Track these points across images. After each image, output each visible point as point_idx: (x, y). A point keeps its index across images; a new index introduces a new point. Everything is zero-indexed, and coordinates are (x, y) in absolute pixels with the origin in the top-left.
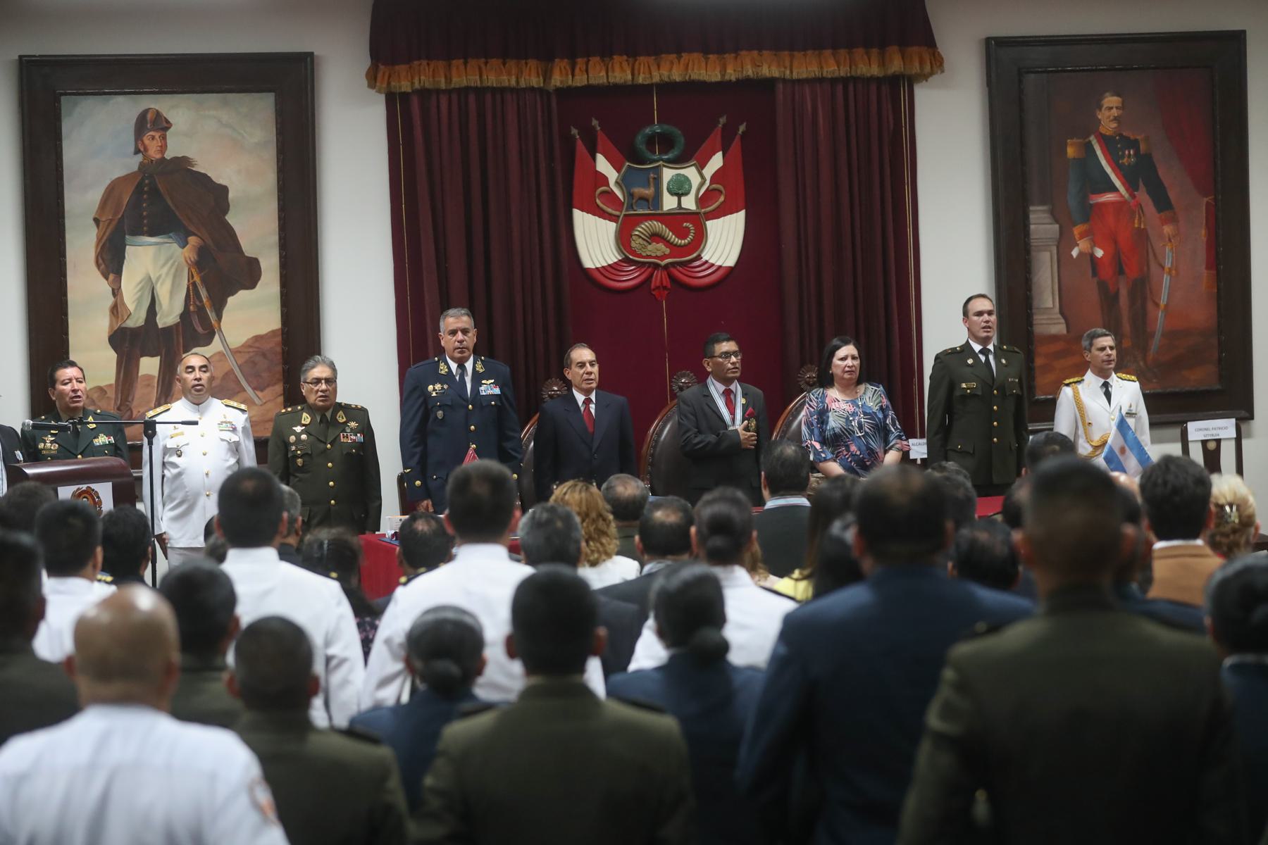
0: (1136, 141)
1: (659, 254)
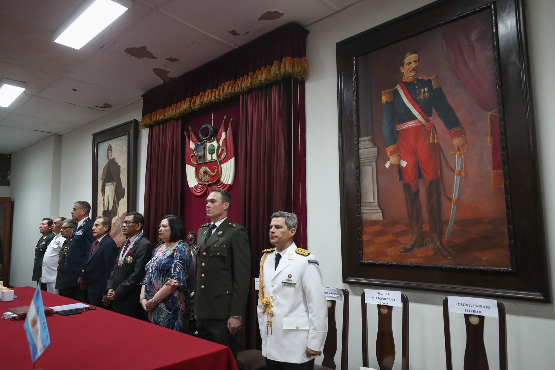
0: (430, 81)
1: (207, 180)
